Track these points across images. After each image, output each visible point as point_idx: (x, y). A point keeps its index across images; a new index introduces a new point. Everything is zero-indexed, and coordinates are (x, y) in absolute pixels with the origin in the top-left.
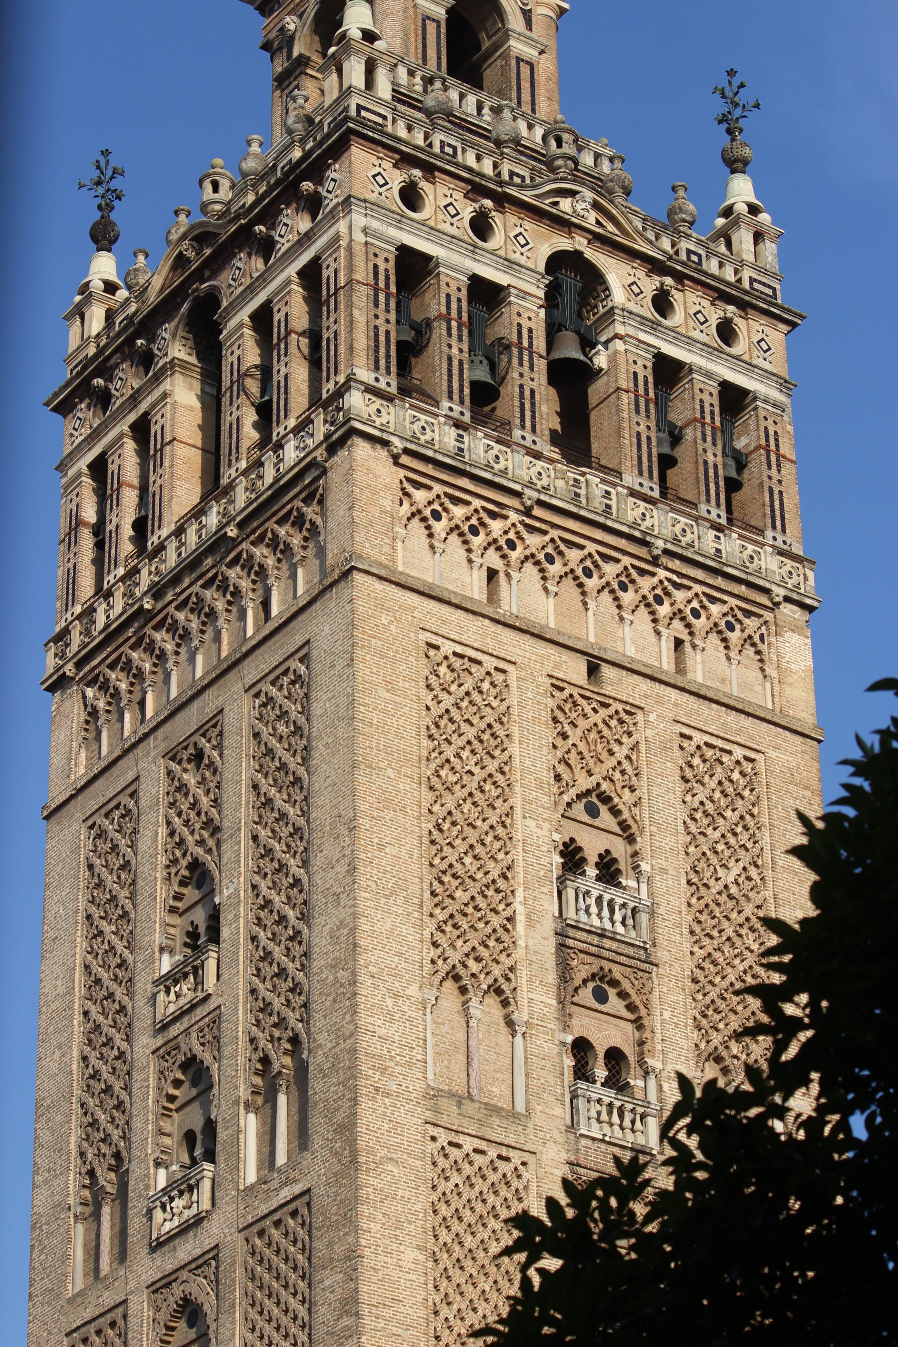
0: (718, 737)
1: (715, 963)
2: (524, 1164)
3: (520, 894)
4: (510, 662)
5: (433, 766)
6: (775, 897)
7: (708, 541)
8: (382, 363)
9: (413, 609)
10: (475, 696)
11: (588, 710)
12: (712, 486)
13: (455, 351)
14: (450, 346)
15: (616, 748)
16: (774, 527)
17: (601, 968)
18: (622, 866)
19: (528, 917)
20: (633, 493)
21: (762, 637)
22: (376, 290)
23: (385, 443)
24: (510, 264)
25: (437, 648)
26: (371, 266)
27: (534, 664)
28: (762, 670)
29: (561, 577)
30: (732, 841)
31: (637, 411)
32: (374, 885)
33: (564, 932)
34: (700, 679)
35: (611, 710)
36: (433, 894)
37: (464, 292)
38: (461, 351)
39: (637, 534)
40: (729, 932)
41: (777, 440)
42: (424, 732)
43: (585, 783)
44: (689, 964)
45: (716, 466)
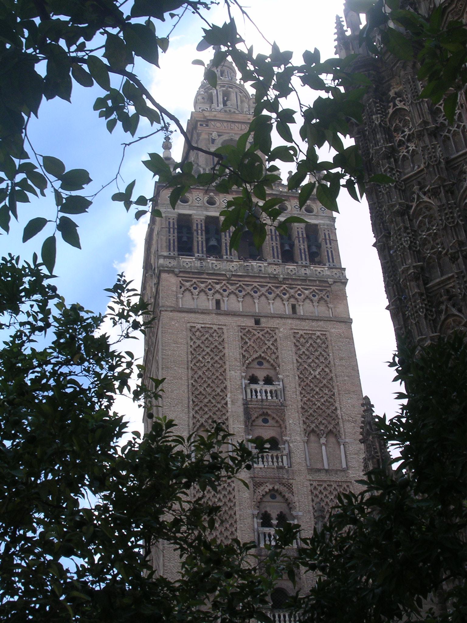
0: (309, 330)
1: (312, 401)
3: (229, 395)
4: (223, 325)
5: (193, 363)
6: (336, 375)
7: (303, 271)
8: (172, 248)
9: (184, 318)
10: (210, 339)
11: (256, 333)
12: (303, 255)
13: (200, 239)
14: (198, 238)
16: (329, 261)
19: (232, 401)
20: (269, 264)
21: (328, 296)
22: (169, 229)
25: (195, 327)
26: (167, 222)
29: (244, 296)
30: (317, 361)
31: (272, 240)
32: (169, 404)
33: (246, 404)
34: (302, 314)
35: (266, 331)
36: (194, 402)
37: (203, 221)
38: (202, 238)
39: (272, 276)
40: (317, 390)
42: (189, 353)
44: (300, 404)
45: (304, 249)
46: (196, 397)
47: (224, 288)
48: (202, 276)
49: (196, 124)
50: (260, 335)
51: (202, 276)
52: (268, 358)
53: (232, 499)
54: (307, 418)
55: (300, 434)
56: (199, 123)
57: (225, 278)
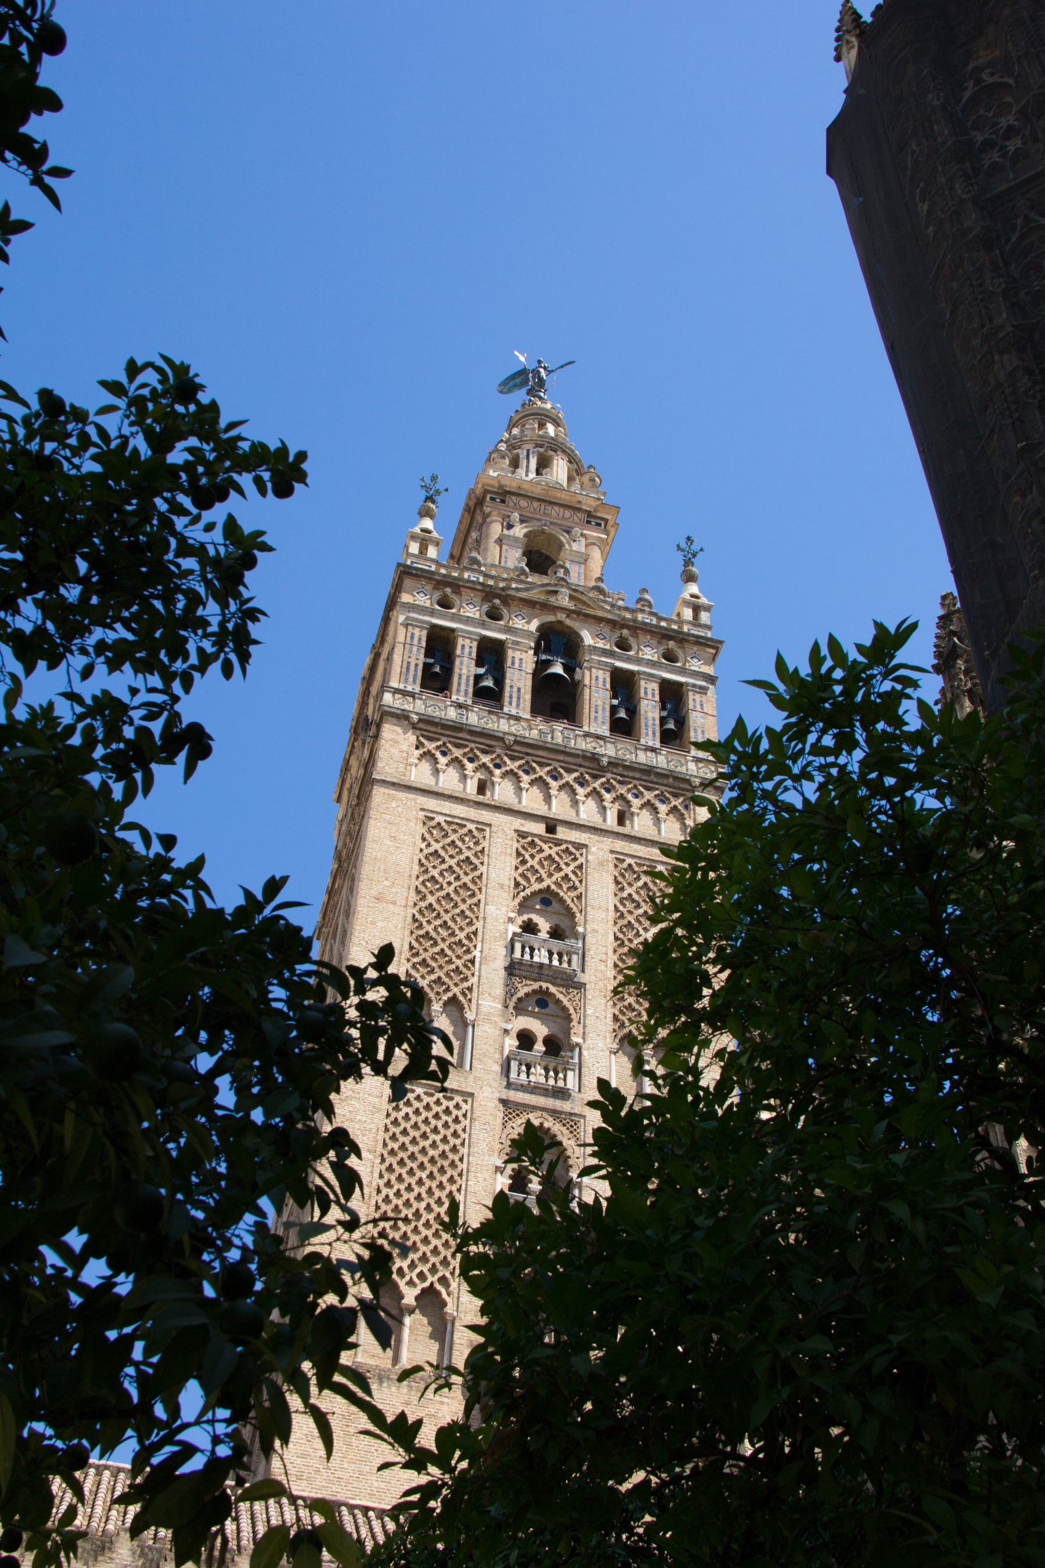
0: (645, 859)
2: (465, 1101)
5: (421, 879)
8: (411, 679)
11: (545, 847)
13: (464, 671)
15: (564, 867)
17: (541, 987)
18: (567, 933)
23: (407, 718)
24: (509, 630)
25: (433, 819)
27: (505, 826)
28: (684, 824)
32: (364, 943)
36: (411, 948)
39: (588, 754)
41: (702, 705)
43: (537, 887)
46: (417, 940)
47: (498, 761)
48: (460, 735)
49: (484, 497)
50: (553, 852)
51: (460, 735)
52: (562, 894)
53: (460, 1132)
54: (621, 1011)
55: (605, 1037)
56: (488, 496)
57: (501, 744)
